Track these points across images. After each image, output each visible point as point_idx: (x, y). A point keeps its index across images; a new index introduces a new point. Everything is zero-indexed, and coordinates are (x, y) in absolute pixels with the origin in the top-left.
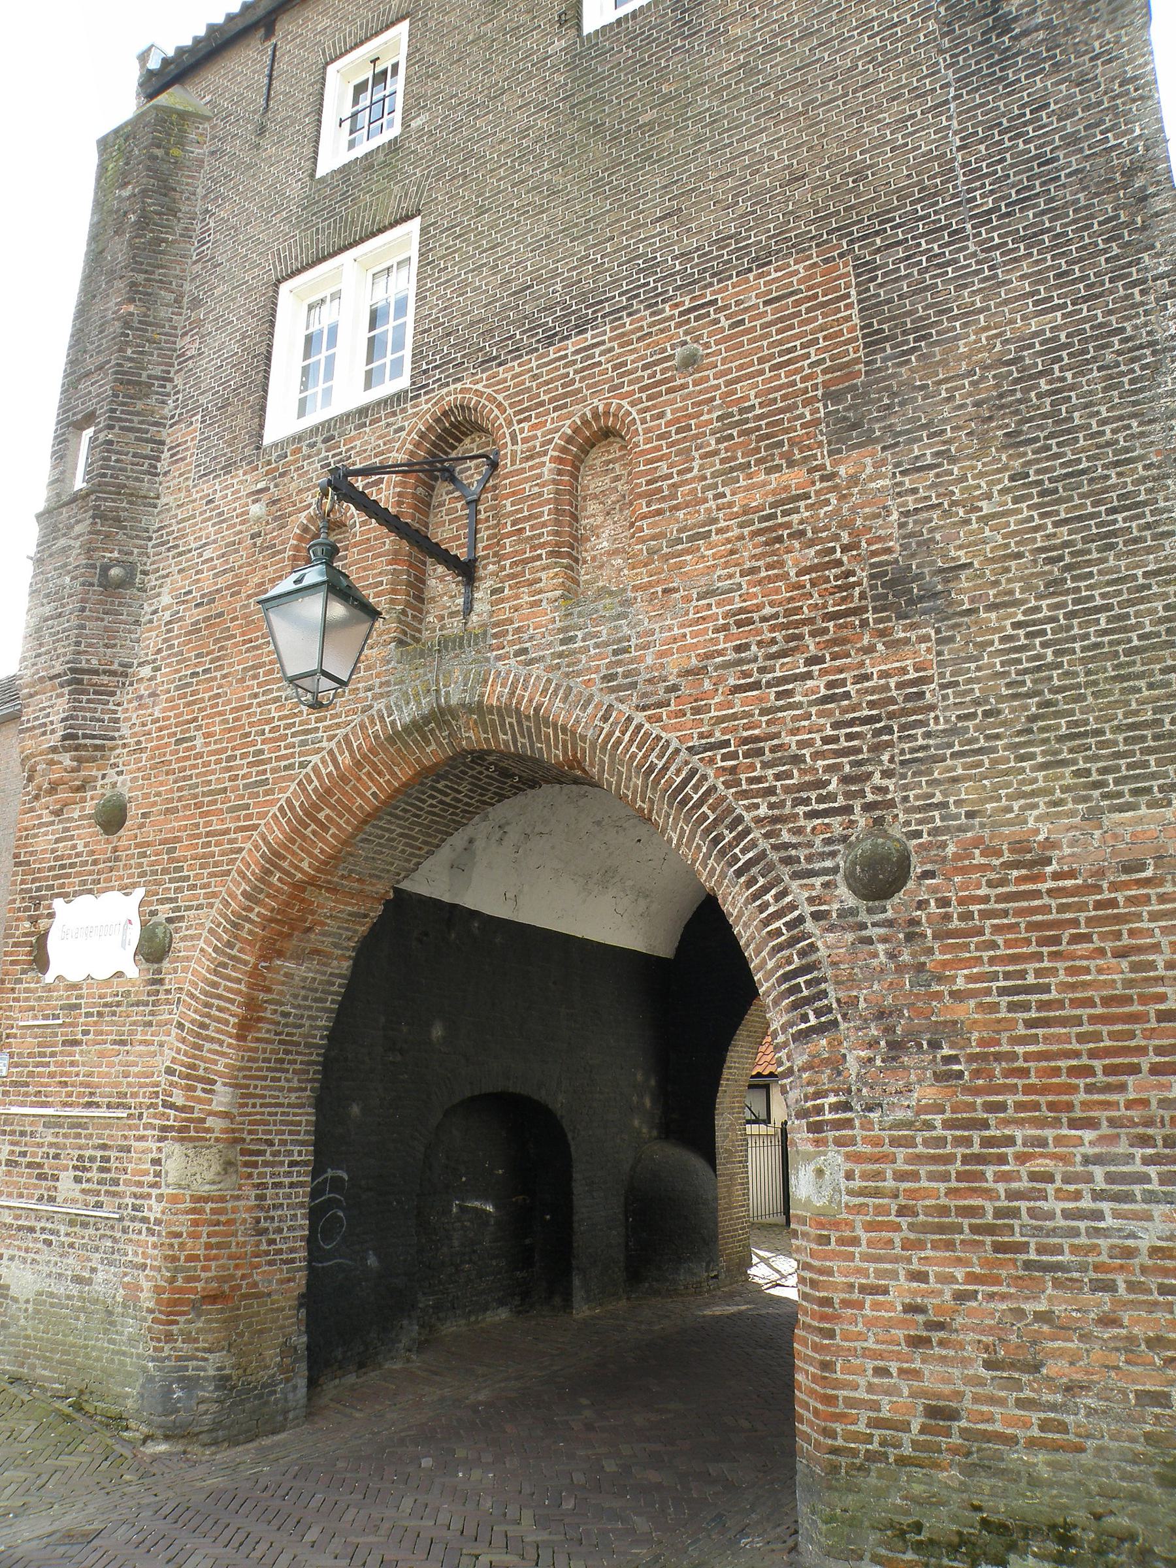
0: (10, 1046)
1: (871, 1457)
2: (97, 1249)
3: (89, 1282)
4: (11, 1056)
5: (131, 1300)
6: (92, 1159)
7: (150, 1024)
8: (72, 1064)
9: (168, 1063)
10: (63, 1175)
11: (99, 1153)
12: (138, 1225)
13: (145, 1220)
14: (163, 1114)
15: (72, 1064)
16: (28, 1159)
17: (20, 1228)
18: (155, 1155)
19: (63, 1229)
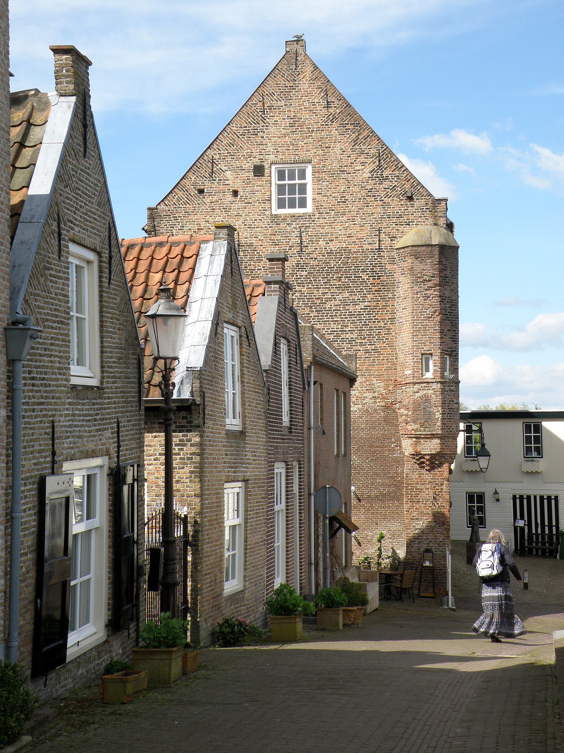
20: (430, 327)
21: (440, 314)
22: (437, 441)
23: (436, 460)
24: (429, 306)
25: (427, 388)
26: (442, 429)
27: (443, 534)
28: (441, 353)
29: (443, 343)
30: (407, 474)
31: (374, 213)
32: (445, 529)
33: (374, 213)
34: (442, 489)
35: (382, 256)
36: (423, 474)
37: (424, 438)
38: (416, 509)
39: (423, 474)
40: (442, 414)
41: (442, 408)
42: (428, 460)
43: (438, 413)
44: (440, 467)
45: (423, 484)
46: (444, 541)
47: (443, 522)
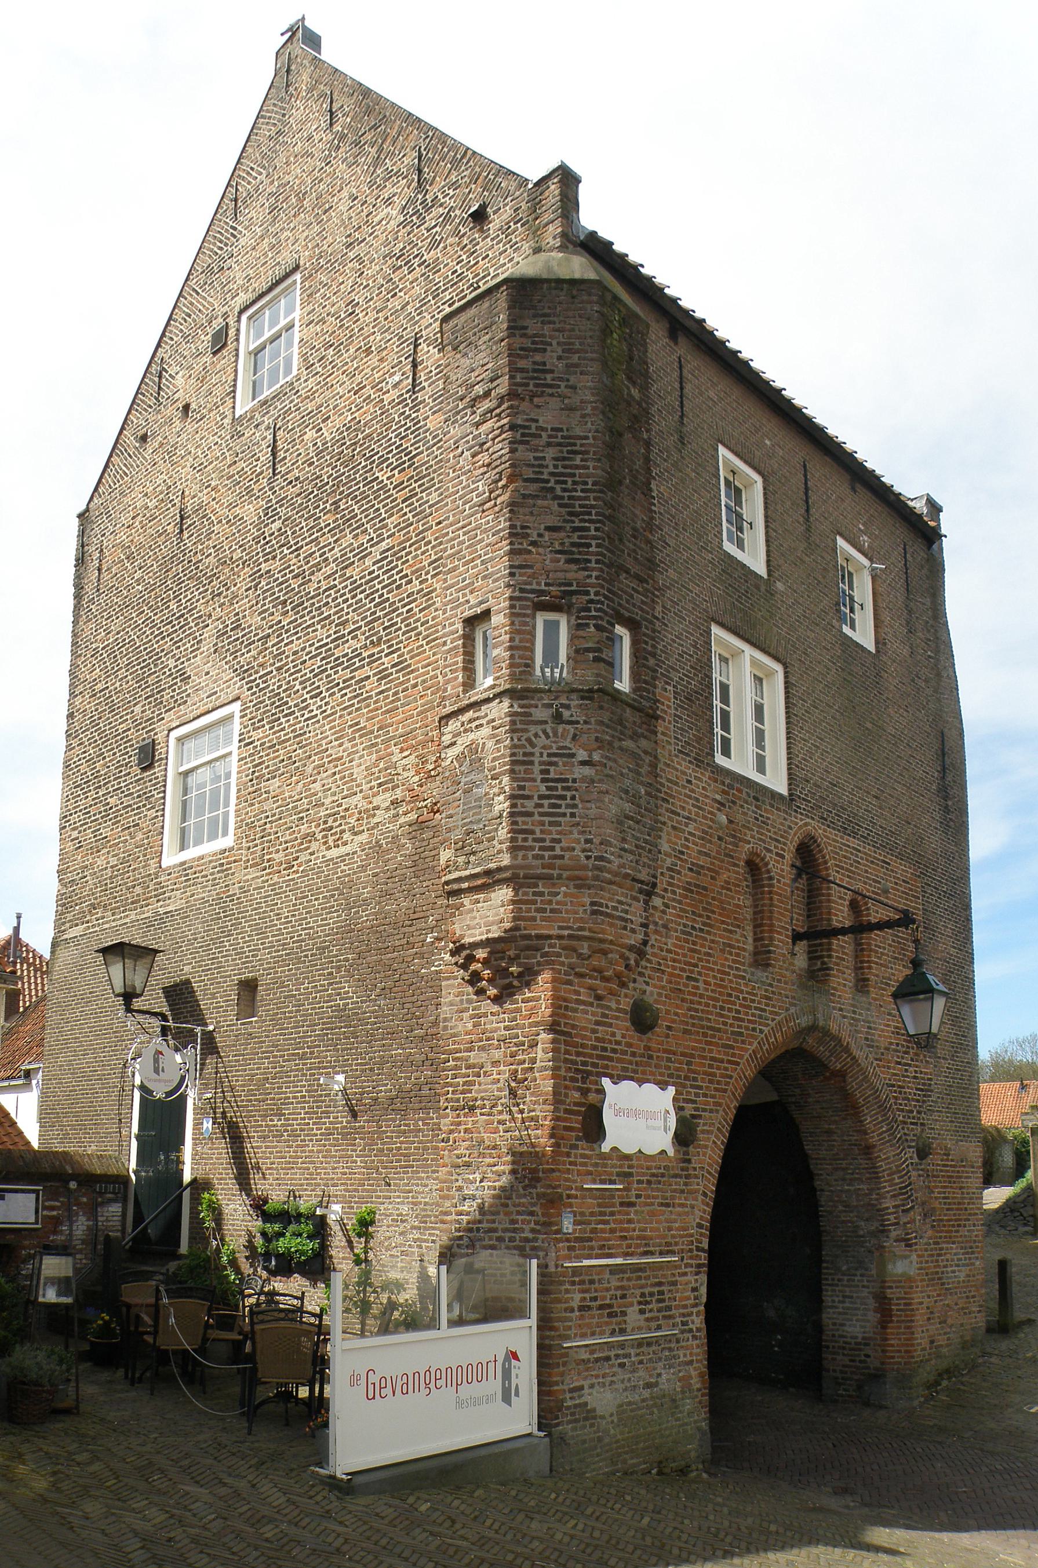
0: (571, 1205)
1: (921, 1361)
2: (660, 1359)
3: (656, 1384)
4: (575, 1214)
5: (687, 1387)
6: (651, 1294)
7: (682, 1192)
8: (630, 1221)
9: (698, 1220)
10: (629, 1310)
11: (656, 1289)
12: (686, 1335)
13: (691, 1331)
14: (697, 1256)
15: (630, 1221)
16: (598, 1303)
17: (597, 1360)
18: (693, 1285)
19: (632, 1352)
20: (485, 531)
21: (511, 479)
22: (504, 894)
23: (512, 960)
24: (482, 470)
25: (474, 725)
26: (513, 849)
27: (532, 1213)
28: (511, 598)
29: (520, 567)
30: (445, 1020)
31: (408, 303)
32: (540, 1196)
33: (408, 303)
34: (533, 1061)
35: (421, 403)
36: (485, 1015)
37: (470, 890)
38: (466, 1131)
39: (485, 1015)
40: (512, 797)
41: (513, 779)
42: (486, 962)
43: (501, 798)
44: (528, 984)
45: (482, 1049)
46: (536, 1240)
47: (535, 1171)
